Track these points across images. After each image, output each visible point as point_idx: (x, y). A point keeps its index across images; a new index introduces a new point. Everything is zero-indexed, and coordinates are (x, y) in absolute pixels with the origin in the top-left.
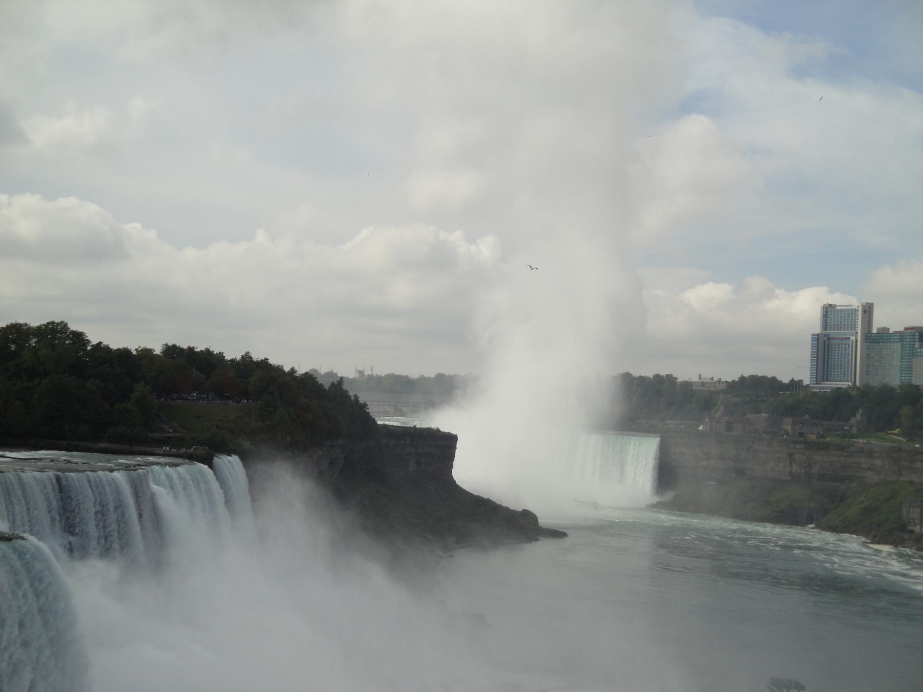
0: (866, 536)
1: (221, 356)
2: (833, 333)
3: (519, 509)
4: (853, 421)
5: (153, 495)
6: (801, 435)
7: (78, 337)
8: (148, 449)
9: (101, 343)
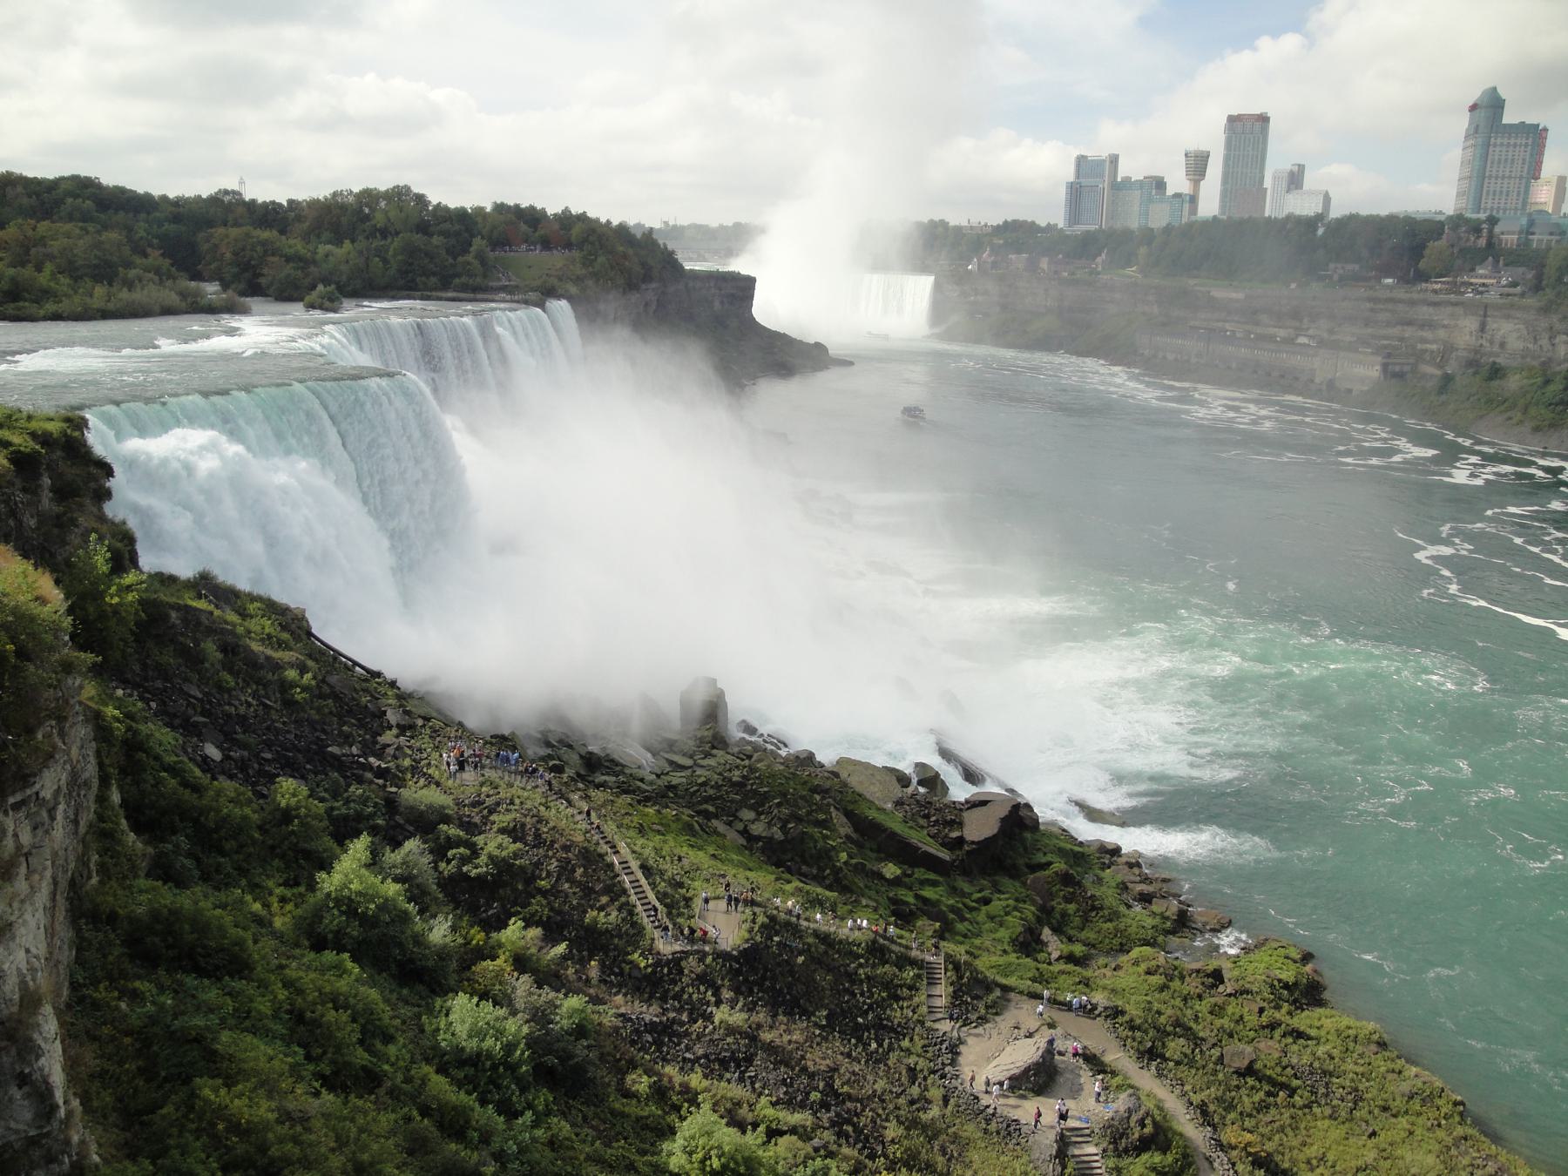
0: (1106, 360)
1: (543, 211)
2: (1084, 182)
4: (1099, 260)
5: (498, 337)
6: (1056, 272)
7: (421, 199)
8: (490, 297)
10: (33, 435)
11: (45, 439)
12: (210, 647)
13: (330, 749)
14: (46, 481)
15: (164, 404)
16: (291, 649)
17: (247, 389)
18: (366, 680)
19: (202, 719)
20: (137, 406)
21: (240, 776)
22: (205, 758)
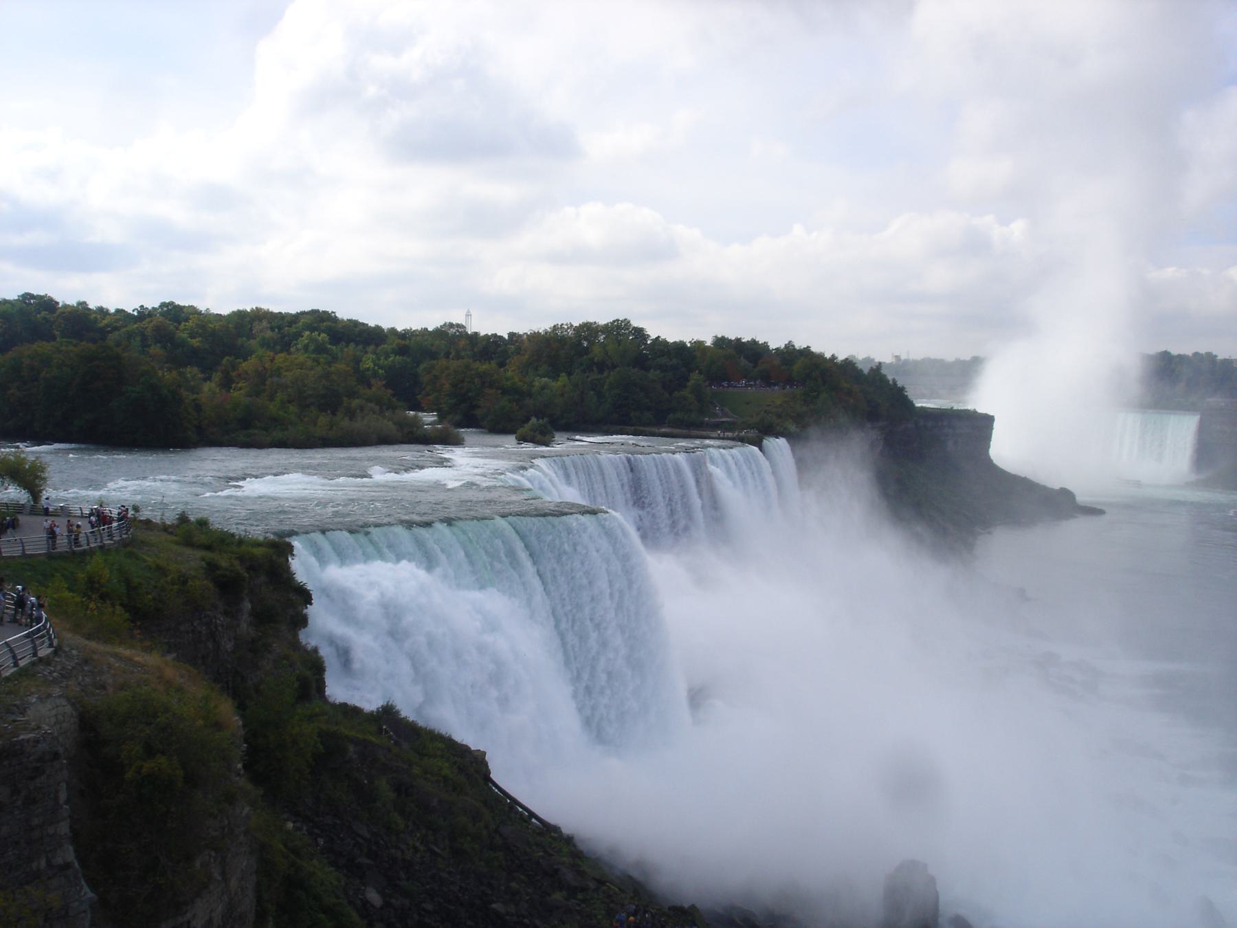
1: (765, 345)
3: (1056, 486)
5: (710, 475)
7: (639, 332)
8: (704, 433)
9: (659, 337)
10: (241, 559)
11: (252, 565)
13: (494, 906)
14: (247, 606)
15: (367, 534)
17: (449, 521)
19: (368, 861)
22: (366, 903)
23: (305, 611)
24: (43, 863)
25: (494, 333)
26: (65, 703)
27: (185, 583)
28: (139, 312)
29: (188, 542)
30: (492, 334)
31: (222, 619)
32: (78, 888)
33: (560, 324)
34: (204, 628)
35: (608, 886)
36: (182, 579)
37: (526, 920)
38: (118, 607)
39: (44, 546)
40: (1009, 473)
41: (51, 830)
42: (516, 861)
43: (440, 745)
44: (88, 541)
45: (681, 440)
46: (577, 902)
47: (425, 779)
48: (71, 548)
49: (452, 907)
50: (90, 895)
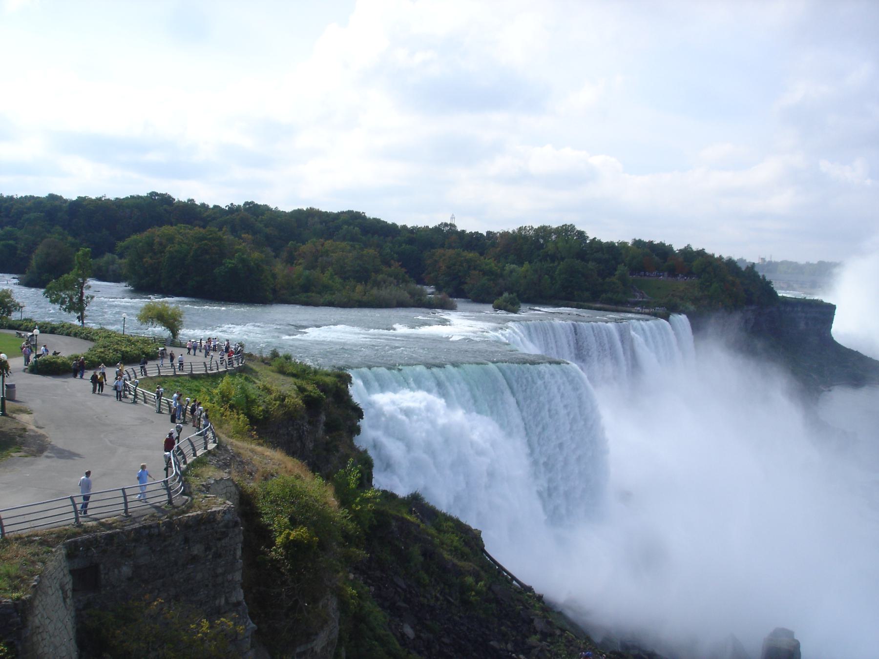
1: (670, 248)
5: (632, 340)
7: (581, 235)
8: (628, 309)
9: (595, 238)
11: (323, 387)
12: (416, 551)
13: (492, 643)
14: (323, 418)
16: (470, 561)
17: (455, 365)
18: (520, 593)
19: (404, 605)
20: (382, 370)
21: (426, 653)
22: (403, 635)
23: (358, 423)
24: (223, 601)
25: (476, 231)
26: (231, 484)
27: (283, 400)
28: (229, 208)
29: (282, 371)
30: (475, 232)
31: (307, 426)
32: (245, 620)
33: (524, 226)
34: (295, 432)
35: (567, 633)
36: (281, 397)
37: (513, 655)
38: (242, 416)
39: (189, 369)
40: (845, 348)
41: (230, 577)
42: (504, 612)
43: (451, 524)
44: (218, 366)
45: (612, 313)
46: (547, 643)
47: (442, 548)
48: (206, 370)
49: (463, 642)
50: (255, 626)
